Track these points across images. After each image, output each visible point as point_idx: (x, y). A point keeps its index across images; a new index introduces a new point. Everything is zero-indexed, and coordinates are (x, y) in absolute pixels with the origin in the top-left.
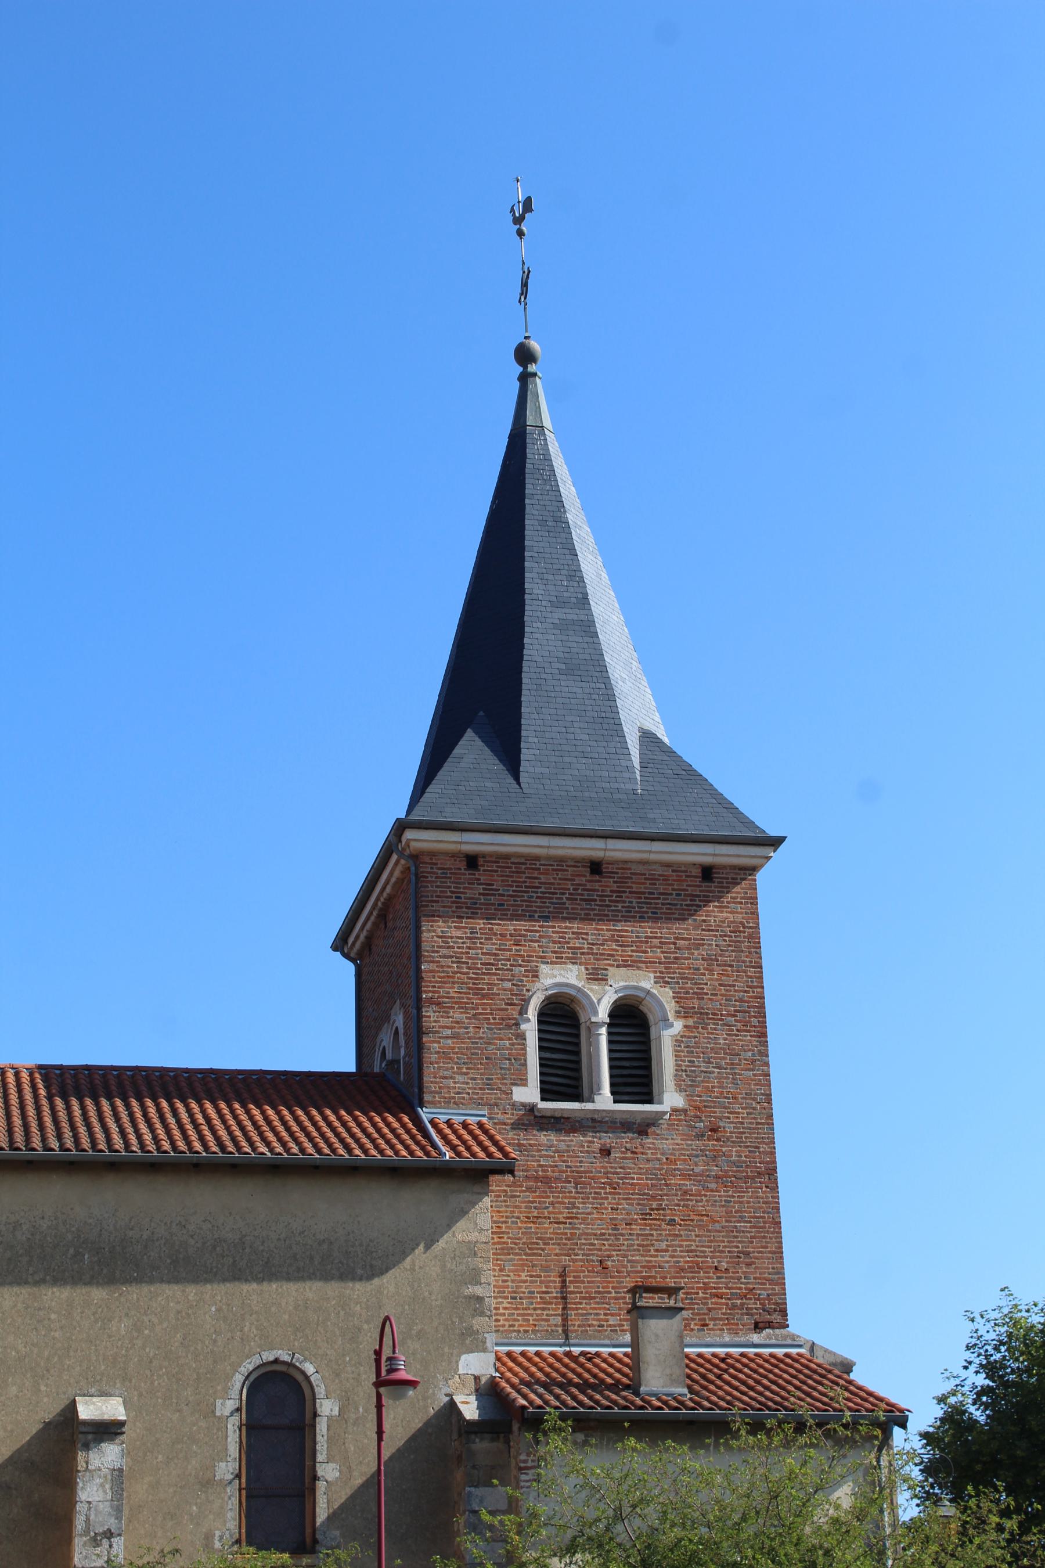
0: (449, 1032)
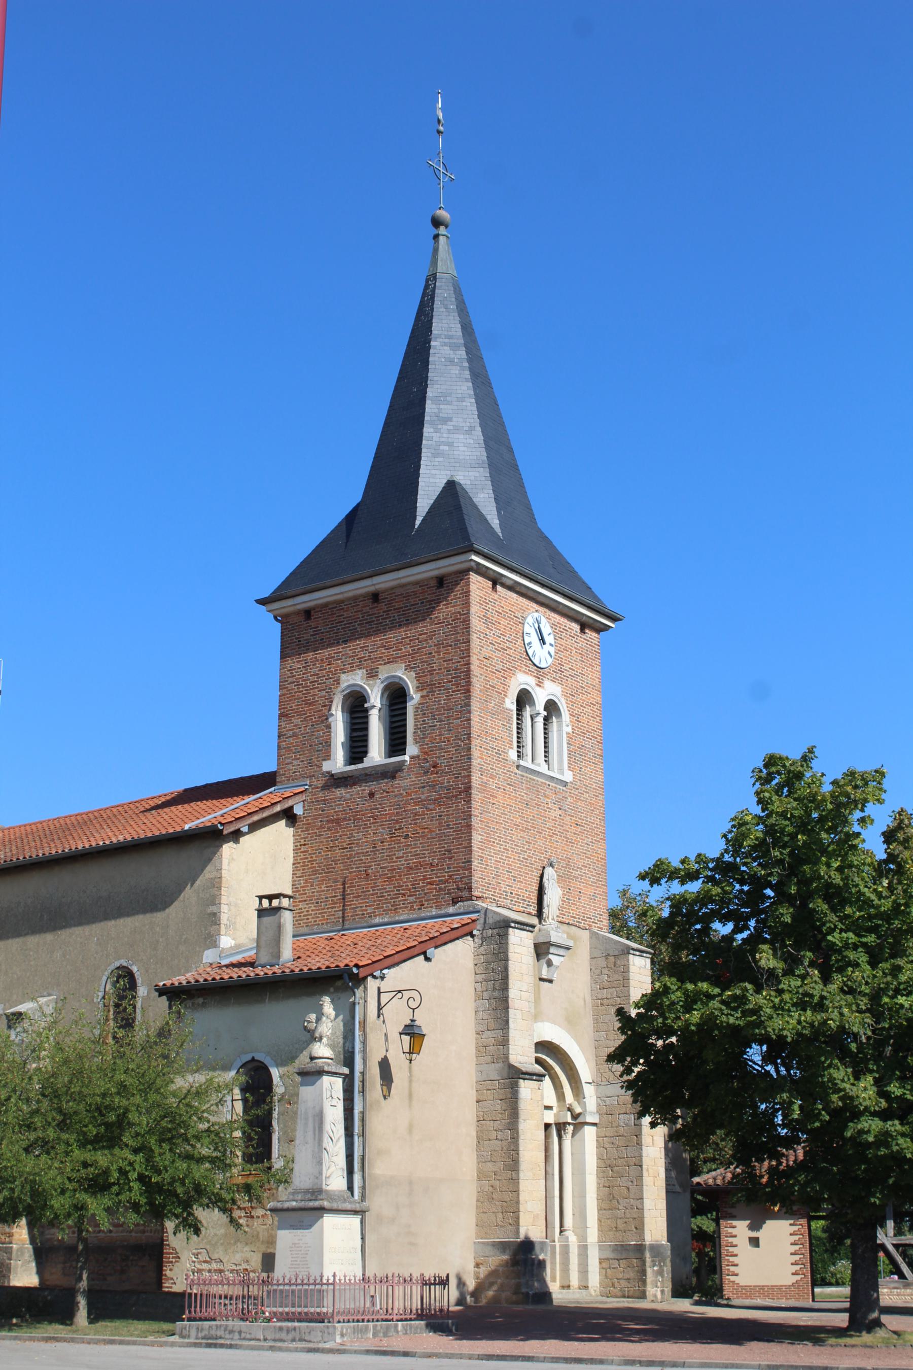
0: (291, 733)
